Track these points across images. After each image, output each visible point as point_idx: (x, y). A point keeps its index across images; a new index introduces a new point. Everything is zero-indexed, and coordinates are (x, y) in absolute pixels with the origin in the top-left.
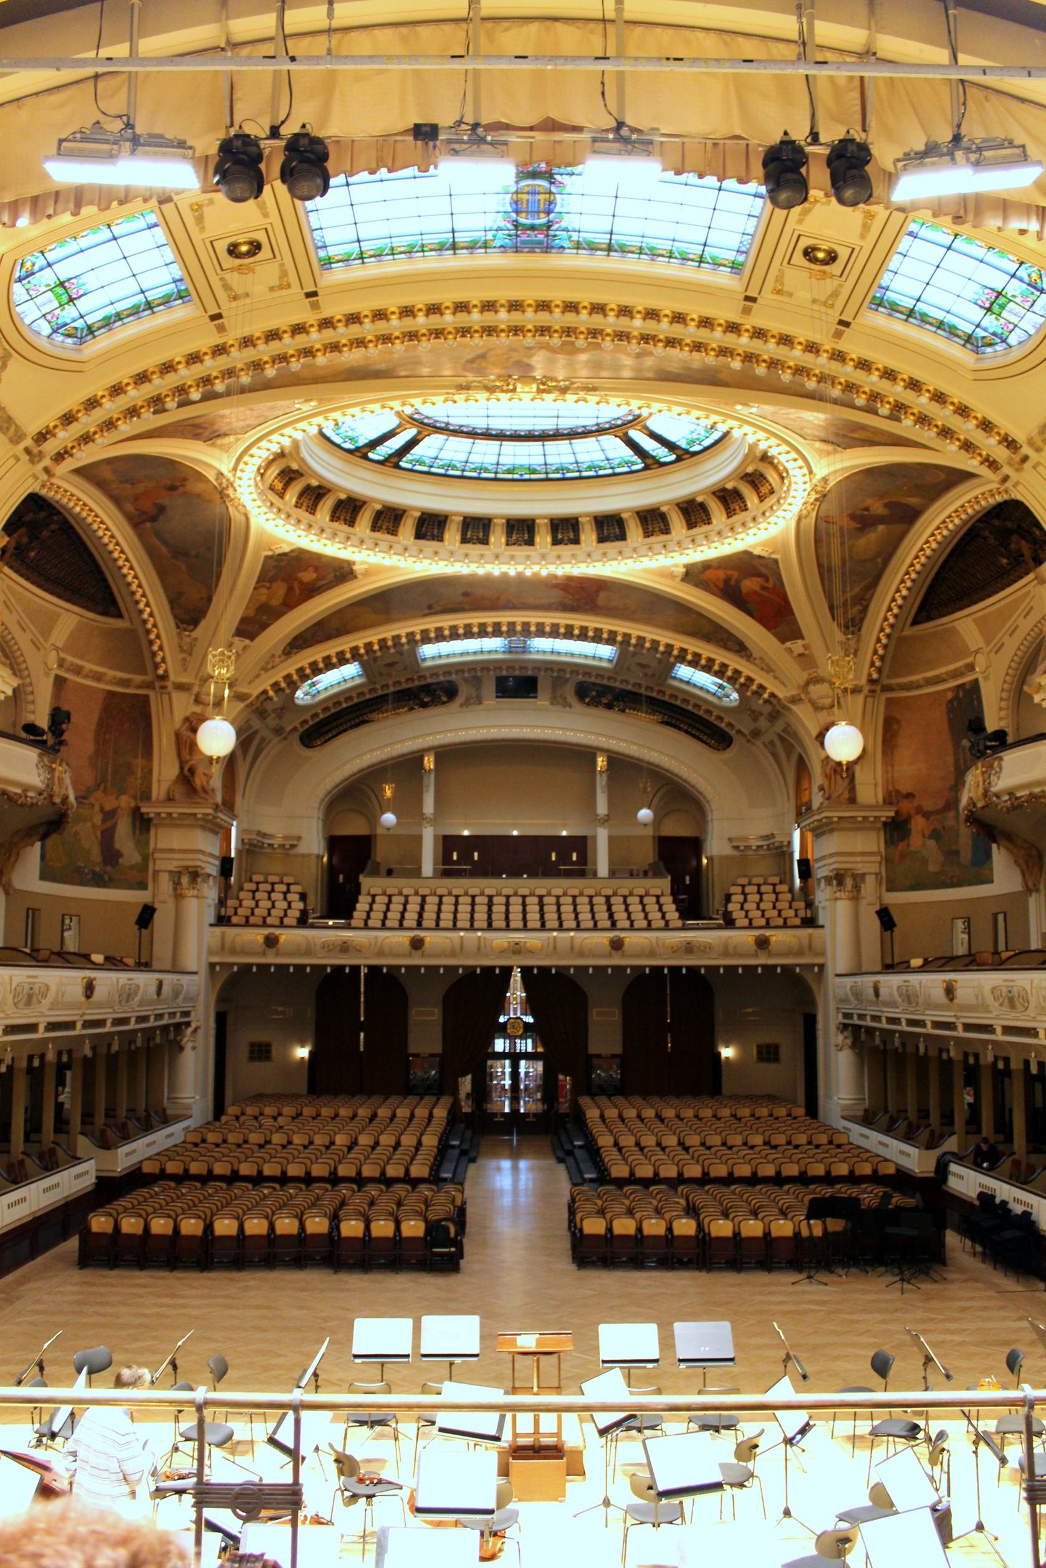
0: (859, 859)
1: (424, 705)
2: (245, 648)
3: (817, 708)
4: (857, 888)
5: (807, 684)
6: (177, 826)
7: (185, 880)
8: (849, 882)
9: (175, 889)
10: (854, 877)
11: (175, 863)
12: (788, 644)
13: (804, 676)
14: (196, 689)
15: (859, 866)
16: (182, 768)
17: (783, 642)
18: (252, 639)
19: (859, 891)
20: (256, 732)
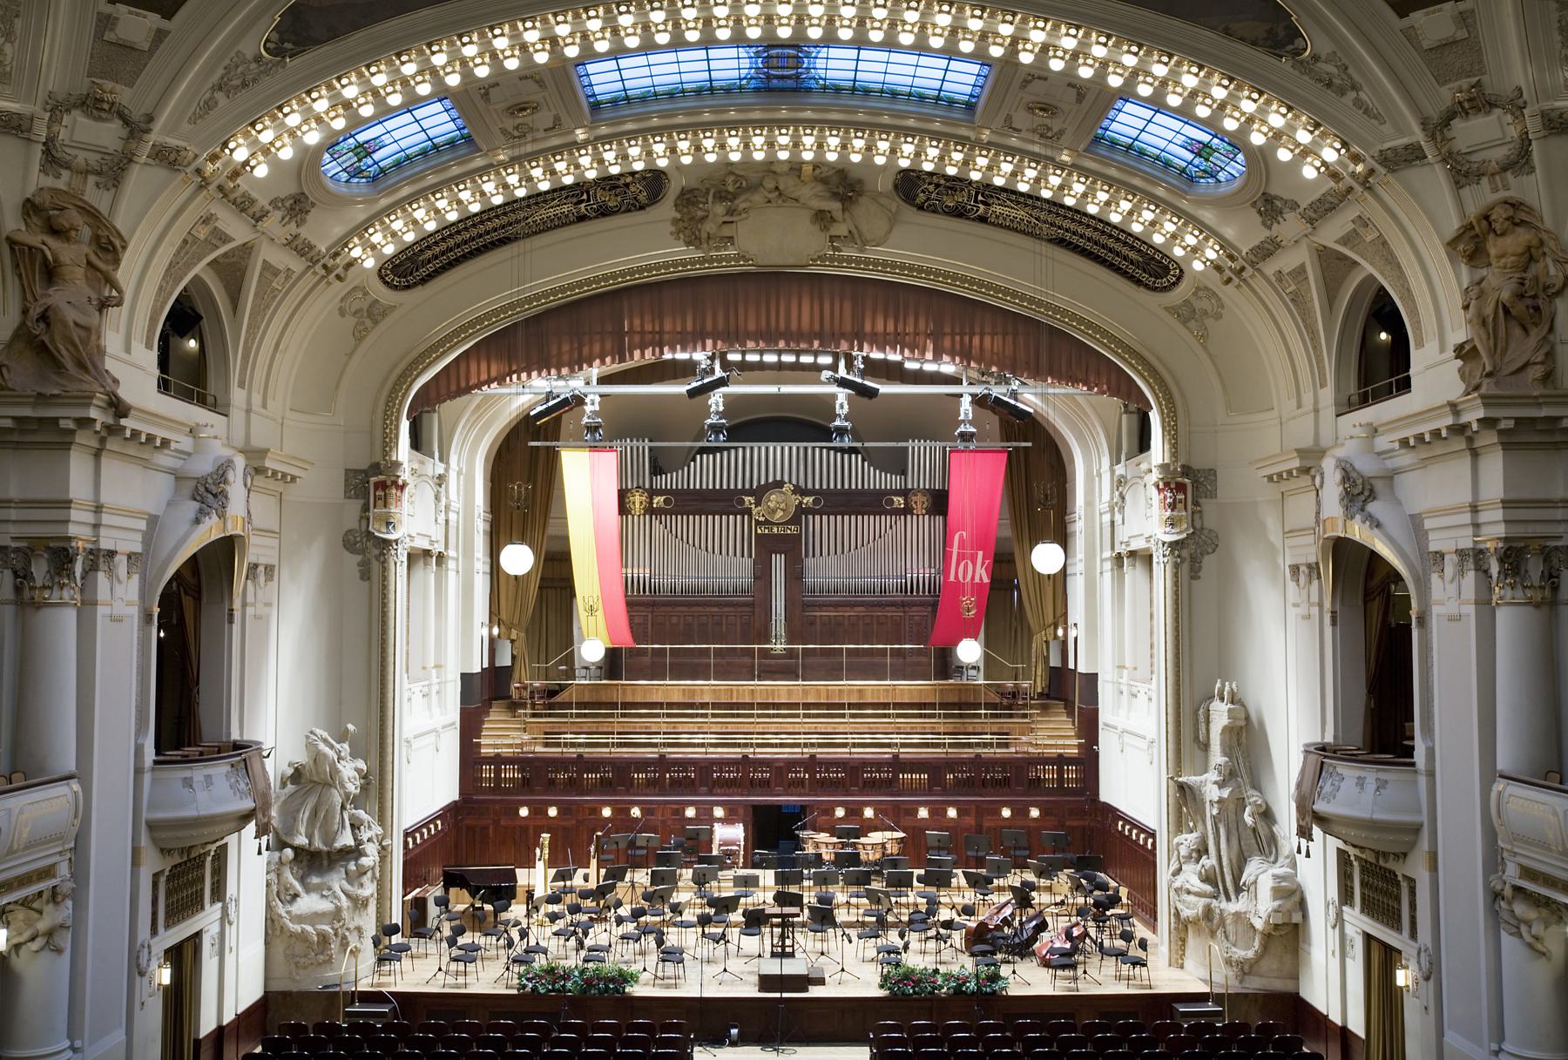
0: (1559, 514)
1: (604, 212)
2: (160, 35)
3: (1463, 174)
4: (1551, 578)
5: (1448, 118)
6: (18, 446)
7: (40, 569)
8: (1535, 568)
9: (18, 589)
10: (1547, 554)
11: (14, 530)
12: (1418, 17)
13: (1447, 95)
14: (42, 133)
15: (1561, 529)
16: (25, 312)
17: (1402, 14)
18: (168, 14)
19: (1555, 589)
20: (247, 249)
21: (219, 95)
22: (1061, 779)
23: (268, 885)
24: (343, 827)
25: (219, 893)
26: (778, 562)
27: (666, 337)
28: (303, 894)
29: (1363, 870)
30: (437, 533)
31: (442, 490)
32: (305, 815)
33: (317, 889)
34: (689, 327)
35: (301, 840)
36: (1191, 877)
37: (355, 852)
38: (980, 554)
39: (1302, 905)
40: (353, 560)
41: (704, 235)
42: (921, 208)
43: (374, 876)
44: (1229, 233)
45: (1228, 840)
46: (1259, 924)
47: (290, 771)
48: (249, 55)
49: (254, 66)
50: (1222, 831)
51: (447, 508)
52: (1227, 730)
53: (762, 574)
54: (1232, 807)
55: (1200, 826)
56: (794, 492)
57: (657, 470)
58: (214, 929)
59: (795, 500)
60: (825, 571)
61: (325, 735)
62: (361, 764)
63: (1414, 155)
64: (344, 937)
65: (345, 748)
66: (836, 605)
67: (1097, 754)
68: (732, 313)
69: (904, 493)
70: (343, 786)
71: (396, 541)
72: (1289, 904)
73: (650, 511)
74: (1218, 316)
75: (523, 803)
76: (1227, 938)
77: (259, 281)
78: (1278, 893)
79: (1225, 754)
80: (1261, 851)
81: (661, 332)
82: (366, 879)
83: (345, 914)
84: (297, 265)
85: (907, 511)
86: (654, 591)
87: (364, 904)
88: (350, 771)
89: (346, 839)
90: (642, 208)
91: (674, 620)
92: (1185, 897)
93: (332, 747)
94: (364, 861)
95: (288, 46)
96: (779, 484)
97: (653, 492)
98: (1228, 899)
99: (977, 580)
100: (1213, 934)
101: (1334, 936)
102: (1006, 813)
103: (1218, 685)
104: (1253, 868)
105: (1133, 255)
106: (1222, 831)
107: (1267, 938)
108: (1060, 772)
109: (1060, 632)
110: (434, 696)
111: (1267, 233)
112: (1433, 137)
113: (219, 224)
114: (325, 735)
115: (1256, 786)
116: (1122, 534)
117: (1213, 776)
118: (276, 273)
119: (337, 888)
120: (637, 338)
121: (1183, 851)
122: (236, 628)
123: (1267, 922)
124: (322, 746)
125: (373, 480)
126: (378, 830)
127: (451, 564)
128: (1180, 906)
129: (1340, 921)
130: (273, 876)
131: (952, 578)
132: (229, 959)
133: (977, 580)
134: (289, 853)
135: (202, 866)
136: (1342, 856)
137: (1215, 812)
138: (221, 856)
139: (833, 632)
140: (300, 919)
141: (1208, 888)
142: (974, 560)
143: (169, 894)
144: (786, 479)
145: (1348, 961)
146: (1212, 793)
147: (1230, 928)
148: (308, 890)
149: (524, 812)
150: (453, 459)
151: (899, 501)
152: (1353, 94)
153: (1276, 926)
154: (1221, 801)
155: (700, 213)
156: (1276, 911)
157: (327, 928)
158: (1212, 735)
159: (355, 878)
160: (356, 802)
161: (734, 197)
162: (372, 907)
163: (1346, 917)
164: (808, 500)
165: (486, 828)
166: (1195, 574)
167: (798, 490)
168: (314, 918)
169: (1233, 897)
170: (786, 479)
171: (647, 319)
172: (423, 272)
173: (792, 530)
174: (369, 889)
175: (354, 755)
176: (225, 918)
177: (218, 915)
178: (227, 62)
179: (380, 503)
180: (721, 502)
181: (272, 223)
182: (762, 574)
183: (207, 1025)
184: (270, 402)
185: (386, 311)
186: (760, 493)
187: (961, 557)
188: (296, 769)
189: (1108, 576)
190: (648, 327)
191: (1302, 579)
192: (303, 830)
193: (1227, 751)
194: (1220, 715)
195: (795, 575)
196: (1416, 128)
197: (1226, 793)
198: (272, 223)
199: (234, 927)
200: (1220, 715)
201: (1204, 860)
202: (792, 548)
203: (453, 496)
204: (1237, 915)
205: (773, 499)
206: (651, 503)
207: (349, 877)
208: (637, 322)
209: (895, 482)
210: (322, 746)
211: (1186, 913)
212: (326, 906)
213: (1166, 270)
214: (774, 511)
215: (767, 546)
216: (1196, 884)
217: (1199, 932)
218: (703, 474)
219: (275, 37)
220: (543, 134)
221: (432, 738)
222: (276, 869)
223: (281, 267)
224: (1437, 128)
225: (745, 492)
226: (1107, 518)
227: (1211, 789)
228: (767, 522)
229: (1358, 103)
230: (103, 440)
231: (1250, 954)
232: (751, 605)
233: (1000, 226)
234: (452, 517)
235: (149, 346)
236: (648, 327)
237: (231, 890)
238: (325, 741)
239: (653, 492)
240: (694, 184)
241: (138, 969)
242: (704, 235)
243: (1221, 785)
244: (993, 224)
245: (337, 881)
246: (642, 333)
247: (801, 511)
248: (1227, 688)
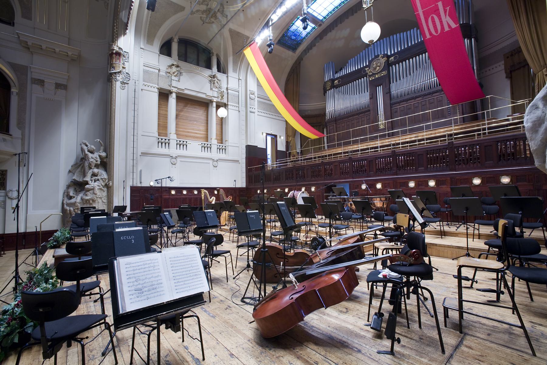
38: (440, 4)
53: (373, 97)
56: (383, 57)
73: (333, 86)
97: (333, 81)
99: (447, 29)
131: (428, 36)
133: (447, 29)
142: (436, 11)
180: (359, 74)
182: (373, 97)
187: (427, 15)
214: (375, 68)
215: (374, 85)
228: (374, 74)
232: (369, 111)
247: (388, 65)
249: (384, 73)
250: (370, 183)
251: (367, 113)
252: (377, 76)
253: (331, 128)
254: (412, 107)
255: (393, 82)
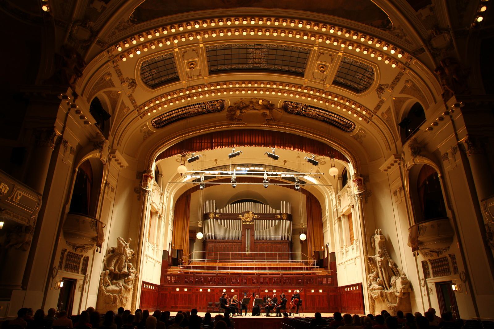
12: (420, 11)
21: (117, 31)
22: (327, 282)
23: (101, 280)
24: (125, 267)
25: (84, 271)
26: (248, 232)
27: (224, 144)
28: (110, 285)
29: (432, 264)
30: (160, 208)
31: (162, 196)
32: (114, 261)
33: (115, 284)
34: (230, 141)
35: (112, 268)
36: (375, 285)
37: (128, 275)
39: (411, 287)
40: (136, 195)
41: (234, 118)
42: (289, 112)
43: (132, 283)
44: (368, 106)
45: (385, 272)
46: (398, 294)
47: (112, 249)
48: (126, 21)
49: (126, 24)
50: (383, 270)
51: (163, 204)
52: (380, 243)
53: (244, 235)
54: (385, 263)
55: (376, 270)
56: (252, 214)
57: (216, 209)
58: (81, 282)
59: (252, 216)
60: (260, 234)
61: (123, 239)
62: (132, 250)
63: (422, 50)
64: (121, 299)
65: (128, 245)
66: (263, 243)
67: (336, 275)
68: (241, 138)
69: (281, 214)
70: (126, 255)
71: (149, 191)
72: (407, 286)
73: (215, 218)
74: (365, 137)
75: (178, 287)
76: (388, 301)
77: (120, 107)
78: (403, 283)
79: (380, 249)
80: (395, 275)
81: (223, 142)
82: (130, 283)
83: (123, 292)
84: (132, 108)
85: (281, 219)
86: (215, 239)
87: (129, 291)
88: (128, 251)
89: (126, 270)
90: (219, 111)
91: (221, 246)
92: (373, 291)
93: (124, 243)
94: (130, 277)
95: (136, 20)
96: (248, 212)
97: (216, 213)
98: (387, 290)
100: (384, 301)
101: (424, 290)
102: (313, 291)
103: (376, 230)
104: (393, 279)
105: (342, 123)
106: (383, 270)
107: (401, 299)
108: (327, 280)
109: (323, 248)
110: (155, 250)
111: (379, 100)
112: (426, 46)
113: (112, 78)
114: (123, 239)
115: (391, 258)
116: (340, 210)
117: (377, 255)
118: (125, 107)
119: (121, 284)
120: (216, 144)
121: (371, 278)
122: (101, 196)
123: (401, 292)
124: (121, 242)
125: (144, 174)
126: (136, 271)
127: (163, 219)
128: (372, 294)
129: (426, 283)
130: (102, 277)
132: (85, 295)
134: (108, 271)
135: (80, 259)
136: (424, 264)
137: (380, 264)
138: (87, 259)
139: (262, 249)
140: (108, 291)
141: (381, 287)
143: (67, 260)
144: (250, 211)
145: (431, 296)
146: (378, 259)
147: (389, 298)
148: (112, 284)
149: (178, 290)
150: (166, 193)
151: (279, 216)
152: (404, 38)
153: (404, 293)
154: (381, 261)
155: (233, 113)
156: (403, 288)
157: (117, 295)
158: (376, 245)
159: (126, 282)
160: (130, 261)
161: (242, 108)
162: (131, 293)
163: (427, 282)
164: (256, 216)
165: (166, 294)
166: (366, 203)
167: (253, 213)
168: (113, 291)
169: (388, 289)
170: (250, 211)
171: (219, 139)
172: (162, 124)
173: (252, 223)
174: (131, 286)
175: (131, 248)
176: (85, 280)
177: (83, 278)
178: (120, 21)
179: (145, 181)
181: (126, 85)
182: (244, 235)
183: (75, 313)
184: (119, 145)
185: (153, 133)
186: (243, 214)
188: (113, 249)
189: (337, 225)
190: (219, 141)
191: (398, 193)
192: (113, 265)
193: (380, 247)
194: (378, 238)
195: (252, 235)
196: (422, 43)
197: (383, 259)
198: (126, 85)
199: (88, 284)
200: (378, 238)
201: (378, 279)
202: (251, 228)
203: (165, 201)
204: (391, 293)
205: (246, 215)
206: (215, 216)
207: (125, 282)
208: (216, 140)
209: (277, 212)
210: (121, 242)
211: (374, 296)
212: (117, 288)
213: (351, 125)
214: (247, 218)
215: (245, 227)
216: (377, 286)
217: (379, 302)
218: (229, 209)
219: (133, 16)
220: (195, 78)
221: (154, 261)
222: (103, 275)
223: (127, 106)
224: (427, 42)
225: (239, 214)
226: (335, 209)
227: (378, 259)
228: (245, 221)
229: (406, 40)
230: (69, 110)
231: (396, 305)
233: (309, 117)
234: (164, 207)
235: (88, 101)
236: (219, 141)
237: (88, 272)
238: (123, 241)
239: (216, 213)
240: (233, 105)
241: (51, 275)
242: (234, 118)
243: (381, 257)
244: (307, 117)
245: (121, 282)
246: (218, 142)
247: (254, 219)
248: (379, 231)
249: (252, 223)
250: (270, 289)
251: (239, 244)
252: (247, 223)
253: (211, 246)
254: (266, 248)
255: (255, 230)
